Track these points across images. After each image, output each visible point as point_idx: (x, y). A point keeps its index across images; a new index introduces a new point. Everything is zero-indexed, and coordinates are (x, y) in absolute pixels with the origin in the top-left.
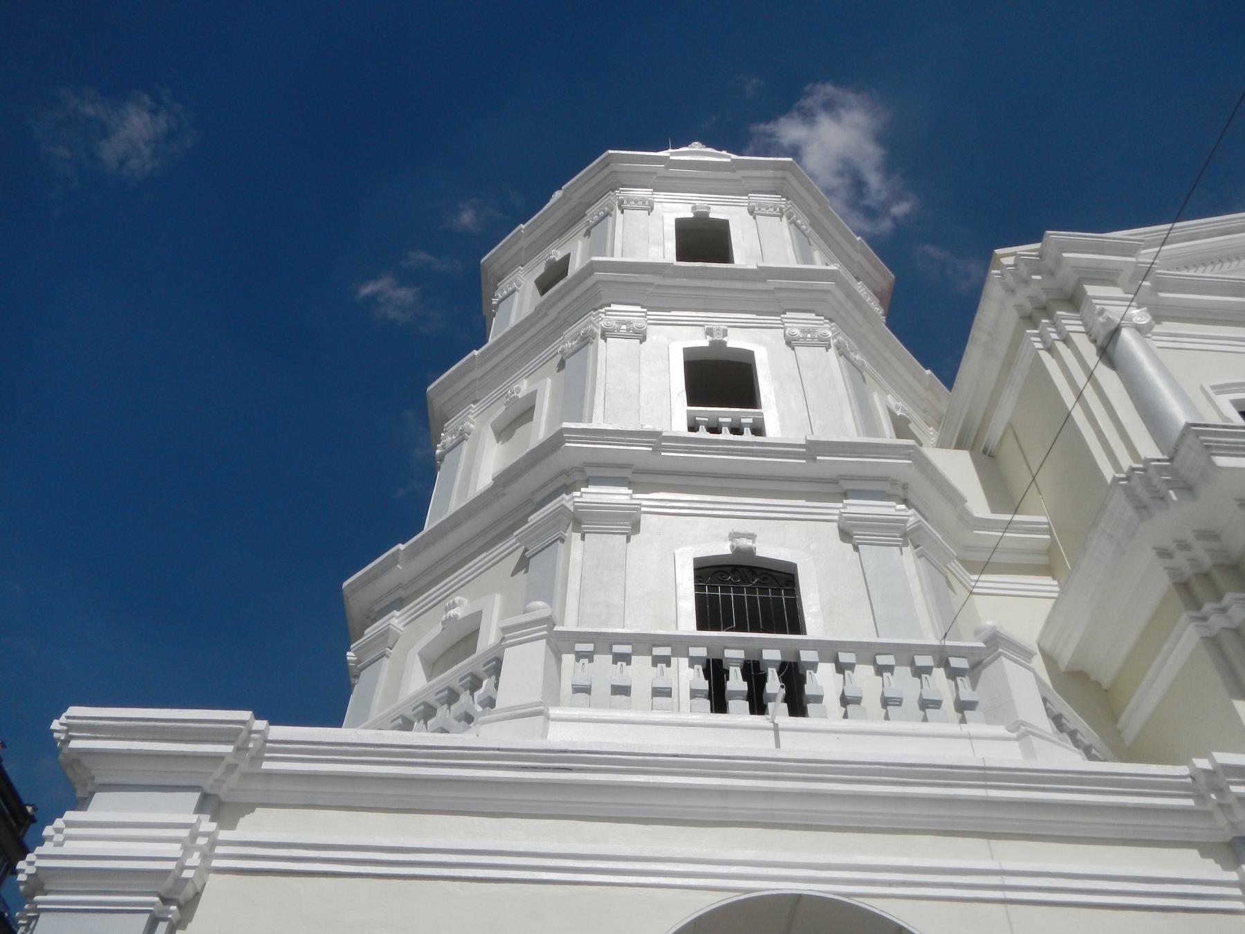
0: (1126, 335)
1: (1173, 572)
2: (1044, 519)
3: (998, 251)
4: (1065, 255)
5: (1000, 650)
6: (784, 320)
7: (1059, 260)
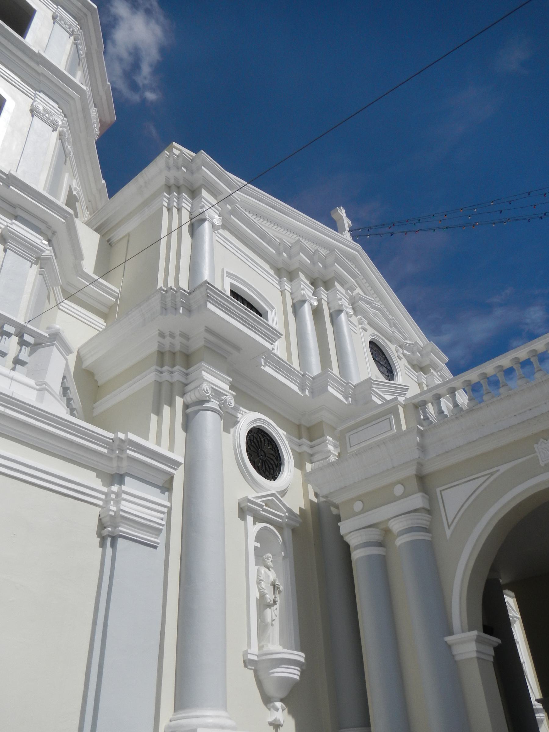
0: (207, 224)
1: (160, 345)
2: (117, 290)
4: (203, 168)
5: (55, 342)
6: (36, 95)
7: (199, 169)
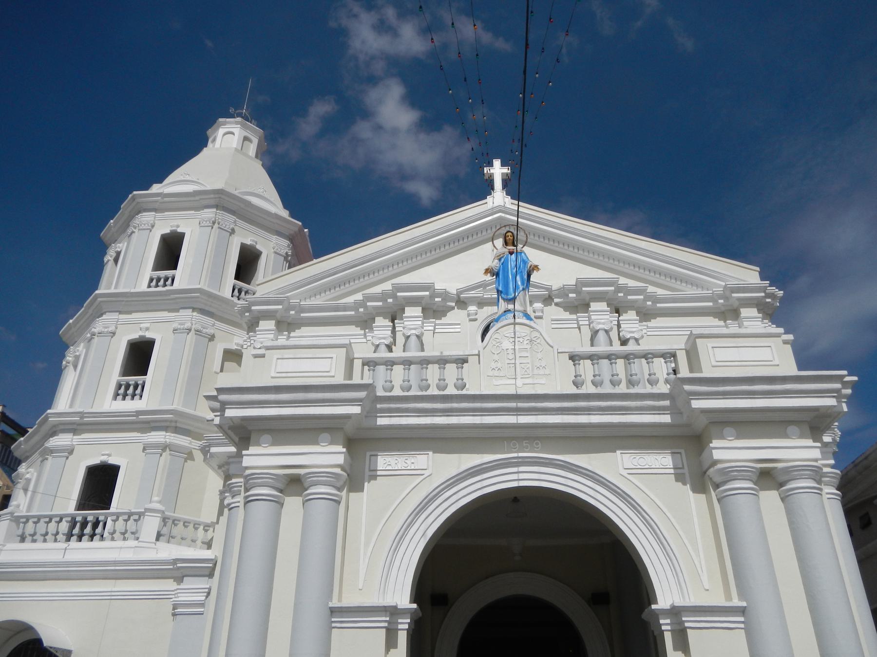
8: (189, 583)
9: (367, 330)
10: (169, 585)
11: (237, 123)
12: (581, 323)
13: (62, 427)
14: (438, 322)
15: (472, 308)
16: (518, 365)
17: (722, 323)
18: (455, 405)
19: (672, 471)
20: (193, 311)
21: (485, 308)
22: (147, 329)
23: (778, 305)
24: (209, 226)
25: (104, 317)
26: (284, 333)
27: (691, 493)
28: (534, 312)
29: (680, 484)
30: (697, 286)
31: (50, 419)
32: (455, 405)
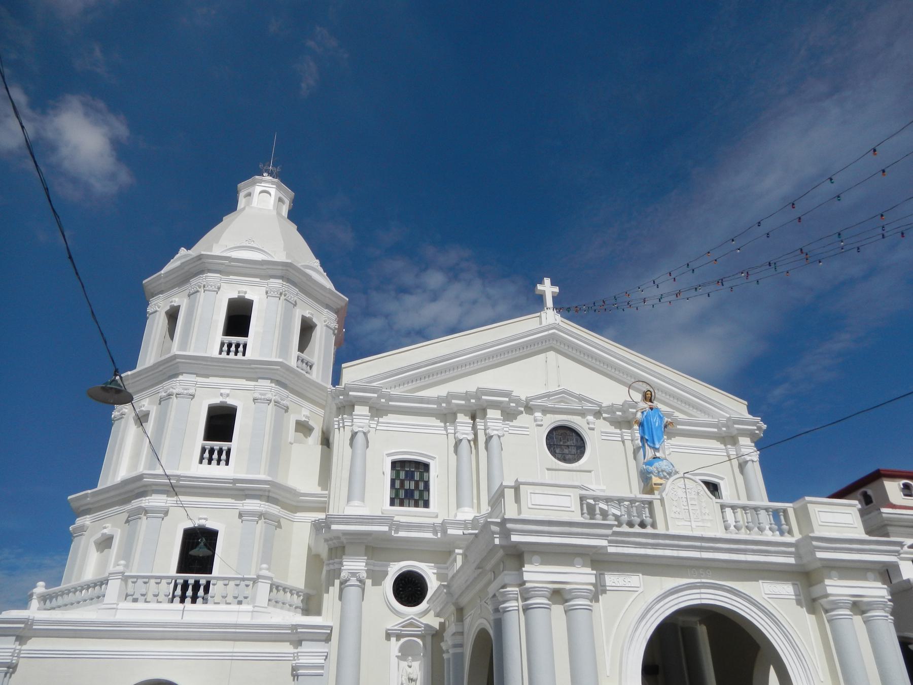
3: (343, 365)
8: (307, 647)
9: (448, 424)
10: (286, 648)
11: (273, 183)
12: (625, 438)
13: (154, 488)
14: (511, 424)
15: (538, 415)
16: (690, 510)
17: (722, 446)
18: (661, 541)
19: (794, 597)
20: (271, 383)
21: (548, 415)
22: (228, 395)
23: (762, 435)
24: (277, 297)
25: (181, 378)
26: (376, 419)
27: (806, 613)
28: (588, 424)
29: (799, 607)
30: (709, 414)
31: (145, 480)
32: (661, 541)
